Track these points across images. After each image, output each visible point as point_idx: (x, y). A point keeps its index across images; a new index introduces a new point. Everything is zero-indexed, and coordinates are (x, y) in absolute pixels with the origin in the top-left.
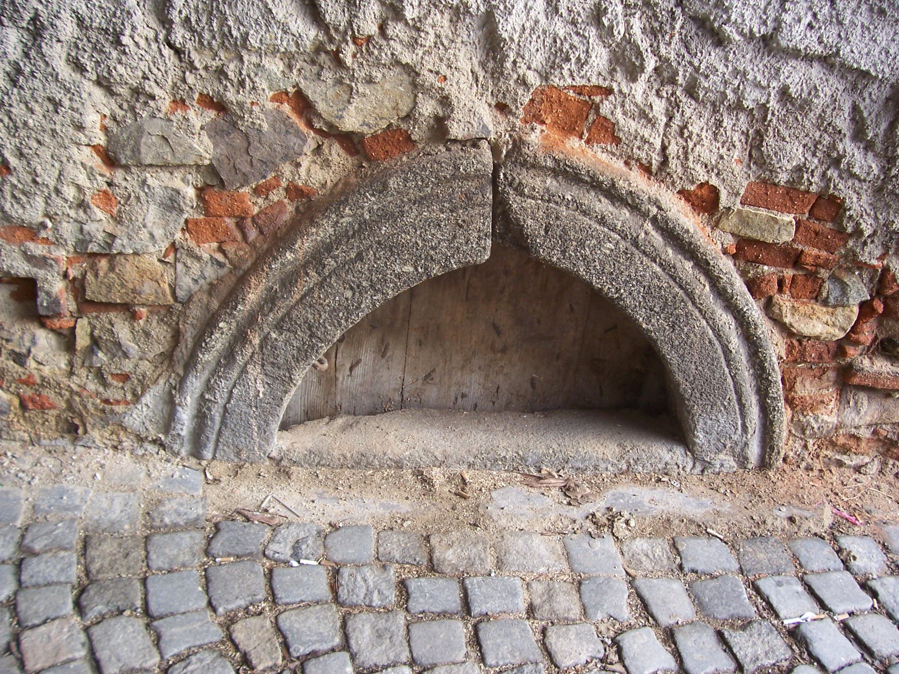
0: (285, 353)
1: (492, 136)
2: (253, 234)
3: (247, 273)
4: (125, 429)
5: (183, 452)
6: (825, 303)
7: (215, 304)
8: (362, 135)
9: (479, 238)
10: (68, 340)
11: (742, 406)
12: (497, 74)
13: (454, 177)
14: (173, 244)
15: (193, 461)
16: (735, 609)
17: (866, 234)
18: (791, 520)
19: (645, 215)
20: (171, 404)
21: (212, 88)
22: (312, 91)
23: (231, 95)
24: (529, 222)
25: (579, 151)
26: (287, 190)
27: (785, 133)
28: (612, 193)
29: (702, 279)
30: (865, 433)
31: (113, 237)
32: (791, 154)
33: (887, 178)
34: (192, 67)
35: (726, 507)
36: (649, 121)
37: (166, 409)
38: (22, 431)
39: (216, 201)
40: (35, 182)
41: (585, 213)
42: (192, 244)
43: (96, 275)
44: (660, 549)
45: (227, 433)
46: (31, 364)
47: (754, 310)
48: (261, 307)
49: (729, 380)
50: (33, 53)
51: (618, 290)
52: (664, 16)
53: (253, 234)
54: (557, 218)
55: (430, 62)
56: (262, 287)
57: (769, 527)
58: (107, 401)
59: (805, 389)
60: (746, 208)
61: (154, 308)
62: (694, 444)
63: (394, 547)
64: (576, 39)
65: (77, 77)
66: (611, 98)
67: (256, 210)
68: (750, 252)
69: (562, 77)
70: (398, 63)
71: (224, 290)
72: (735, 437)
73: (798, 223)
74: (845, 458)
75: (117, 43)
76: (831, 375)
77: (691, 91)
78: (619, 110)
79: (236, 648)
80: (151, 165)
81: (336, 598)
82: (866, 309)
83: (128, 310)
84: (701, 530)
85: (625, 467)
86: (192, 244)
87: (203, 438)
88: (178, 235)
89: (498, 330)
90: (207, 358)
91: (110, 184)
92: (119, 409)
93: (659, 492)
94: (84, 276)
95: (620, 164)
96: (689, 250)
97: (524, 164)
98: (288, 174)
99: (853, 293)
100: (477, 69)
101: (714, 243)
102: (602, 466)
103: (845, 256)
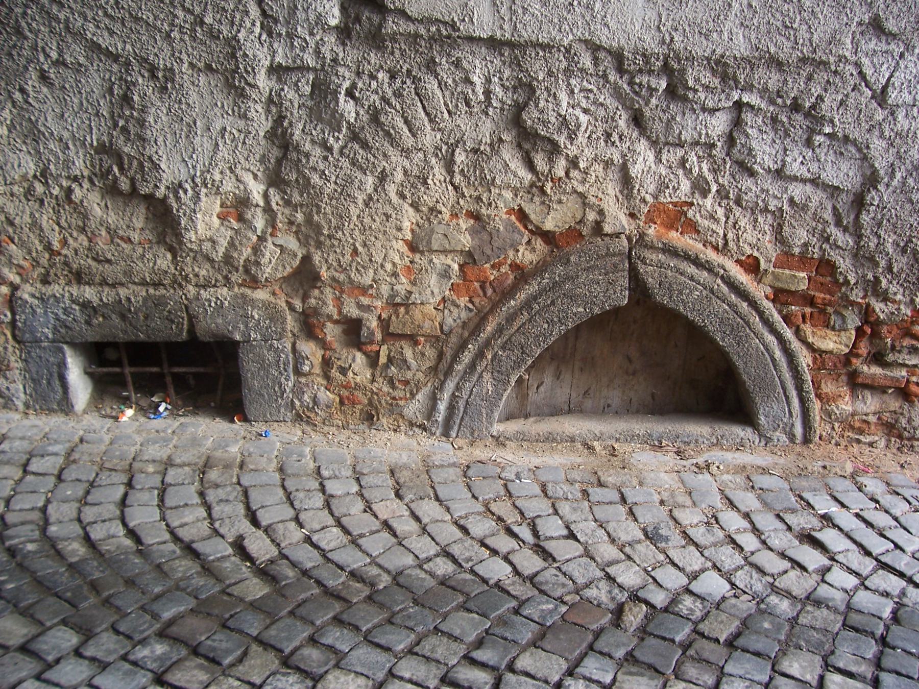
0: (507, 364)
1: (627, 232)
2: (490, 292)
3: (487, 314)
4: (403, 417)
5: (438, 434)
6: (833, 329)
7: (466, 334)
8: (555, 232)
9: (622, 290)
10: (373, 360)
11: (787, 397)
12: (629, 196)
13: (607, 254)
14: (444, 298)
15: (444, 439)
16: (786, 505)
17: (852, 282)
18: (824, 467)
19: (717, 275)
20: (434, 399)
21: (473, 207)
22: (528, 208)
23: (484, 211)
24: (650, 280)
25: (675, 237)
26: (510, 266)
27: (795, 224)
28: (696, 262)
29: (754, 313)
30: (872, 419)
31: (410, 293)
32: (800, 236)
33: (859, 248)
34: (463, 196)
35: (782, 461)
36: (716, 220)
37: (430, 403)
38: (338, 420)
39: (470, 272)
40: (371, 260)
41: (681, 274)
42: (455, 297)
43: (398, 317)
44: (740, 479)
45: (467, 419)
46: (350, 374)
47: (788, 334)
48: (494, 335)
49: (777, 379)
50: (379, 189)
51: (703, 321)
52: (720, 162)
53: (490, 292)
54: (666, 277)
55: (593, 191)
56: (495, 322)
57: (810, 470)
58: (394, 398)
59: (828, 388)
60: (777, 270)
61: (428, 337)
62: (759, 424)
63: (576, 475)
64: (672, 176)
65: (401, 201)
66: (693, 208)
67: (492, 278)
68: (782, 298)
69: (665, 197)
70: (576, 192)
71: (472, 325)
72: (785, 420)
73: (809, 278)
74: (861, 438)
75: (425, 183)
76: (844, 378)
77: (738, 202)
78: (698, 214)
79: (493, 514)
80: (436, 251)
81: (546, 495)
82: (859, 331)
83: (413, 339)
84: (765, 471)
85: (715, 441)
86: (455, 297)
87: (452, 422)
88: (447, 293)
89: (630, 361)
90: (459, 368)
91: (411, 262)
92: (401, 403)
93: (738, 455)
94: (390, 318)
95: (700, 246)
96: (744, 295)
97: (646, 246)
98: (511, 256)
99: (849, 321)
100: (618, 194)
101: (760, 291)
102: (701, 440)
103: (841, 298)
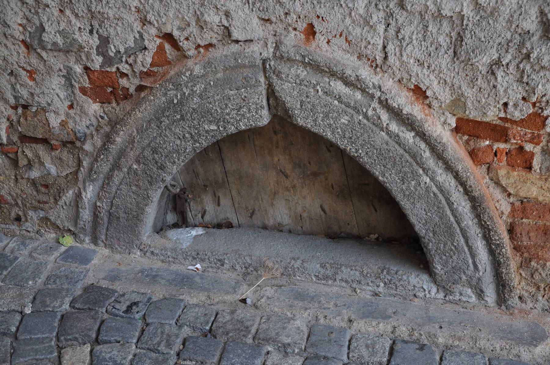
9: (257, 109)
19: (372, 96)
24: (289, 99)
43: (26, 119)
54: (307, 97)
62: (435, 274)
